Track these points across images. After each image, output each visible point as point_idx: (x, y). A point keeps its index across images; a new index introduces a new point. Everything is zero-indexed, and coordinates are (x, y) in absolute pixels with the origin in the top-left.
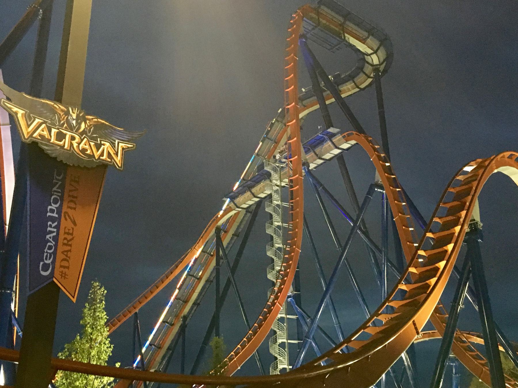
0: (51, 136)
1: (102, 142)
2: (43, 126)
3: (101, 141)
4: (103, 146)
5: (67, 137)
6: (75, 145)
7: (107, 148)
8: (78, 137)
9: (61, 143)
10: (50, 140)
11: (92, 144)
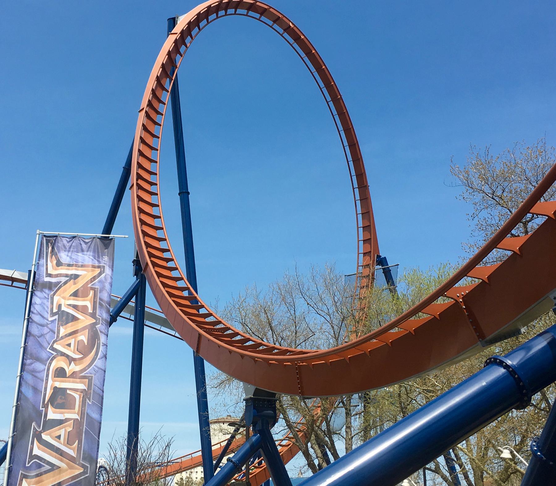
0: (67, 420)
1: (55, 310)
2: (45, 437)
3: (53, 314)
4: (63, 308)
5: (60, 384)
7: (64, 298)
8: (54, 363)
9: (77, 396)
10: (75, 420)
11: (63, 331)
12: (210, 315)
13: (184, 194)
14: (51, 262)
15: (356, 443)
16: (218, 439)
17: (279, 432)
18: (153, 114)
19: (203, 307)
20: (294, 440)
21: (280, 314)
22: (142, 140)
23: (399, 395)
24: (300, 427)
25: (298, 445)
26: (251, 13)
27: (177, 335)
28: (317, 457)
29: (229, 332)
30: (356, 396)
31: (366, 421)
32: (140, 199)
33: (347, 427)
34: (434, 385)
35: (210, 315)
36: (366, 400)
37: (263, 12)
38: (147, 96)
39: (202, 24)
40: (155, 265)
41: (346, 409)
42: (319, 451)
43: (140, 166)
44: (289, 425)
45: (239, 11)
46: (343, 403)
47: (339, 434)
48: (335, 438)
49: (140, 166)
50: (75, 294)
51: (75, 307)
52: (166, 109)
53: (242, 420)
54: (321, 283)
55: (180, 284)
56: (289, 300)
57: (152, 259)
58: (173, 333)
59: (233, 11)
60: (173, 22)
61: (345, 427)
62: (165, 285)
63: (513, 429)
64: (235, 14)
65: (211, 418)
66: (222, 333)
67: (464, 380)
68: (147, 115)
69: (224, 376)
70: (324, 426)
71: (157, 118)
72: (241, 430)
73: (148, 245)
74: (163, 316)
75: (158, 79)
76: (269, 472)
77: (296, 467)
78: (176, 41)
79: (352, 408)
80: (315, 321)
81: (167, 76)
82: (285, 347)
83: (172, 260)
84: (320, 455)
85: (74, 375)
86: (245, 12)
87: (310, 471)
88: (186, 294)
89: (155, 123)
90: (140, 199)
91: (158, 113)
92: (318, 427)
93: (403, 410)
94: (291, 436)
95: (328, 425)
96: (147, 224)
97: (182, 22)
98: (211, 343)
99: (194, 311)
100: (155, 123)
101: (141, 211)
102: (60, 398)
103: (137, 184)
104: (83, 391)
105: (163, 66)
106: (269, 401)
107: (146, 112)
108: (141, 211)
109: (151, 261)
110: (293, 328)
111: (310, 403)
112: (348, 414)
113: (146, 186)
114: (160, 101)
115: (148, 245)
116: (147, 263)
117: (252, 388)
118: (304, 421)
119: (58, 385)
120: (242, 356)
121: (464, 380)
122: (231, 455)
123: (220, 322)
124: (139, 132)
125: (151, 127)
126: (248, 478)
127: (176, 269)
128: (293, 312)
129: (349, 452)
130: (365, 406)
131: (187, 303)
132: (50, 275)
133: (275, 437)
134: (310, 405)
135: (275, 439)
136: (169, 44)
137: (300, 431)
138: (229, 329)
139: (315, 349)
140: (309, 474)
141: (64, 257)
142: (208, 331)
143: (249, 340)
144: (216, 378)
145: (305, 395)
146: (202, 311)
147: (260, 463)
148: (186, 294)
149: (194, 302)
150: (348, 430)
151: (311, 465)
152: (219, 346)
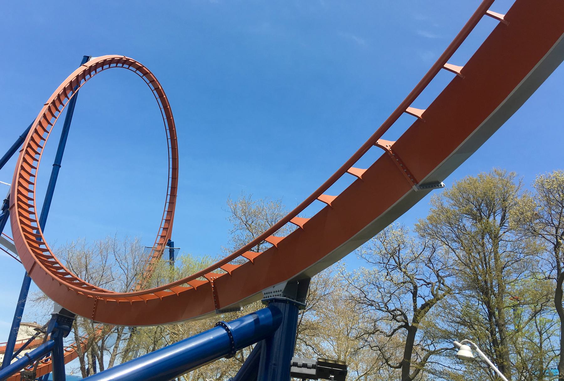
12: (47, 250)
13: (57, 166)
15: (118, 362)
16: (23, 336)
17: (68, 341)
18: (53, 109)
19: (44, 243)
20: (76, 349)
21: (95, 262)
22: (40, 123)
23: (156, 333)
24: (83, 340)
25: (78, 353)
26: (138, 72)
27: (18, 258)
28: (88, 364)
29: (57, 265)
30: (127, 328)
31: (129, 345)
32: (25, 160)
33: (115, 347)
34: (179, 331)
35: (47, 250)
36: (133, 331)
37: (146, 74)
38: (54, 97)
39: (105, 67)
40: (19, 206)
41: (119, 335)
42: (91, 360)
43: (32, 139)
44: (77, 339)
45: (131, 68)
46: (118, 330)
47: (108, 350)
48: (105, 352)
49: (32, 139)
52: (64, 110)
53: (45, 327)
54: (129, 249)
55: (33, 224)
56: (104, 253)
57: (20, 203)
58: (15, 255)
59: (127, 66)
60: (87, 59)
61: (113, 346)
62: (22, 222)
63: (218, 369)
64: (128, 68)
65: (23, 321)
66: (50, 264)
67: (198, 331)
68: (49, 109)
69: (42, 294)
70: (100, 343)
71: (56, 113)
72: (41, 334)
73: (19, 192)
74: (13, 243)
75: (65, 89)
76: (52, 367)
77: (72, 368)
78: (85, 71)
79: (122, 335)
80: (117, 272)
81: (71, 89)
82: (91, 284)
83: (33, 207)
84: (91, 362)
86: (135, 70)
87: (81, 372)
88: (34, 232)
89: (53, 115)
90: (25, 160)
91: (57, 110)
92: (96, 343)
93: (155, 343)
94: (75, 345)
95: (103, 343)
96: (24, 179)
97: (93, 61)
98: (41, 268)
99: (37, 245)
100: (53, 115)
101: (23, 168)
103: (26, 150)
105: (71, 82)
106: (69, 319)
107: (49, 106)
108: (23, 168)
109: (18, 204)
110: (101, 273)
111: (96, 325)
112: (119, 338)
113: (32, 152)
114: (61, 103)
115: (19, 192)
116: (14, 204)
117: (60, 307)
118: (87, 337)
120: (61, 284)
121: (198, 331)
122: (29, 351)
123: (52, 257)
124: (40, 117)
125: (49, 117)
126: (35, 369)
127: (34, 213)
128: (104, 262)
129: (111, 367)
130: (131, 335)
131: (34, 238)
133: (65, 344)
134: (95, 327)
135: (64, 345)
136: (80, 70)
137: (83, 343)
138: (57, 263)
139: (110, 290)
140: (80, 375)
142: (42, 262)
143: (69, 274)
144: (36, 295)
145: (95, 320)
146: (42, 247)
147: (46, 360)
148: (34, 232)
149: (39, 237)
150: (115, 349)
151: (82, 368)
152: (47, 273)
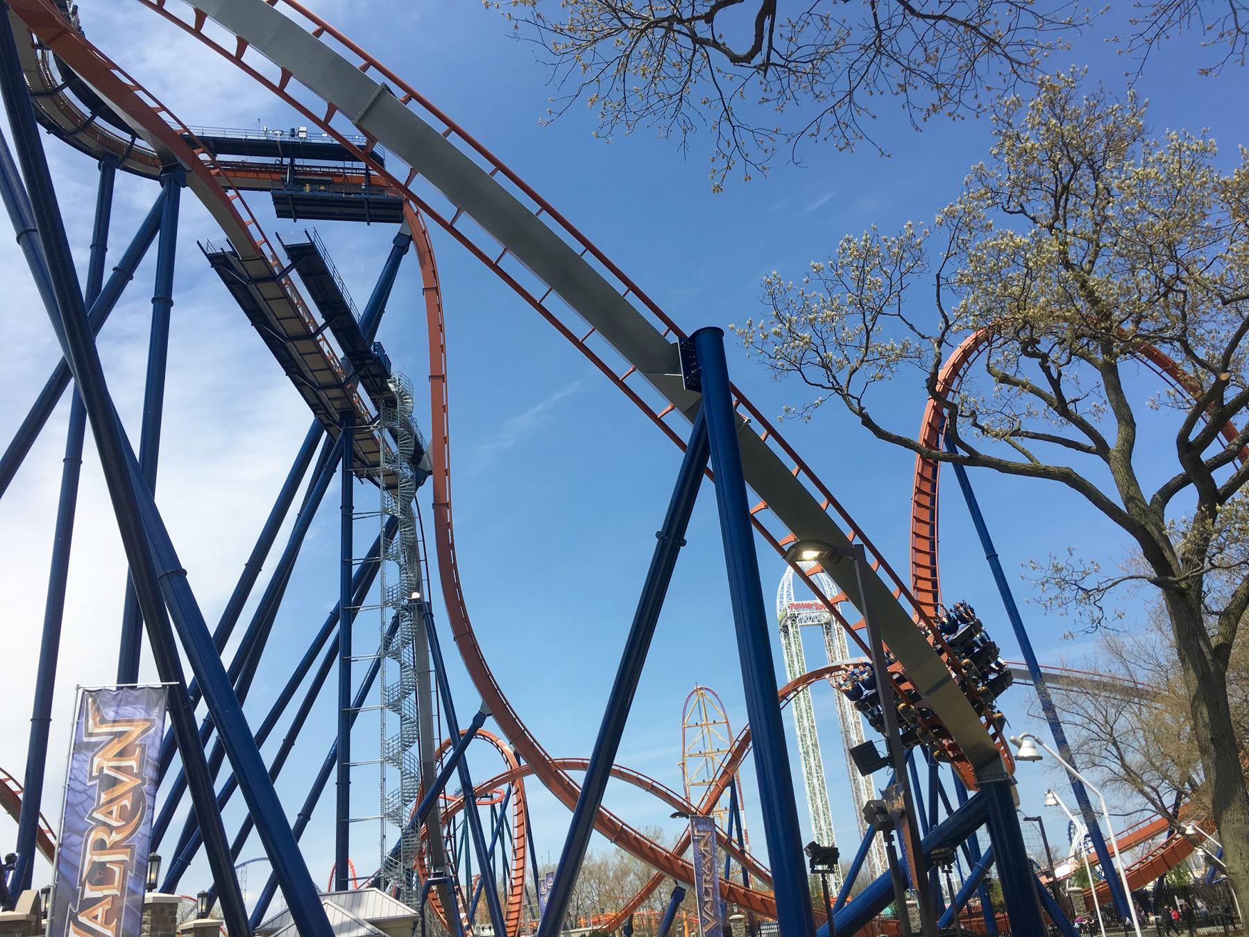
0: (105, 897)
1: (95, 774)
2: (82, 919)
3: (92, 778)
4: (106, 771)
6: (115, 837)
7: (110, 760)
8: (93, 835)
9: (117, 870)
10: (114, 897)
14: (94, 720)
50: (121, 754)
51: (118, 769)
85: (115, 846)
102: (102, 874)
104: (122, 862)
119: (97, 858)
132: (91, 735)
141: (110, 714)
